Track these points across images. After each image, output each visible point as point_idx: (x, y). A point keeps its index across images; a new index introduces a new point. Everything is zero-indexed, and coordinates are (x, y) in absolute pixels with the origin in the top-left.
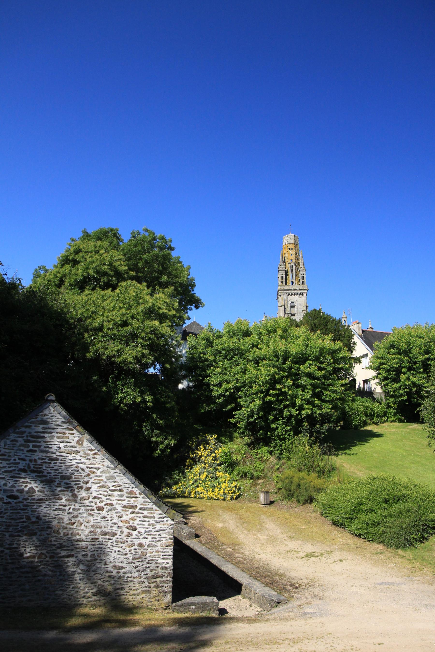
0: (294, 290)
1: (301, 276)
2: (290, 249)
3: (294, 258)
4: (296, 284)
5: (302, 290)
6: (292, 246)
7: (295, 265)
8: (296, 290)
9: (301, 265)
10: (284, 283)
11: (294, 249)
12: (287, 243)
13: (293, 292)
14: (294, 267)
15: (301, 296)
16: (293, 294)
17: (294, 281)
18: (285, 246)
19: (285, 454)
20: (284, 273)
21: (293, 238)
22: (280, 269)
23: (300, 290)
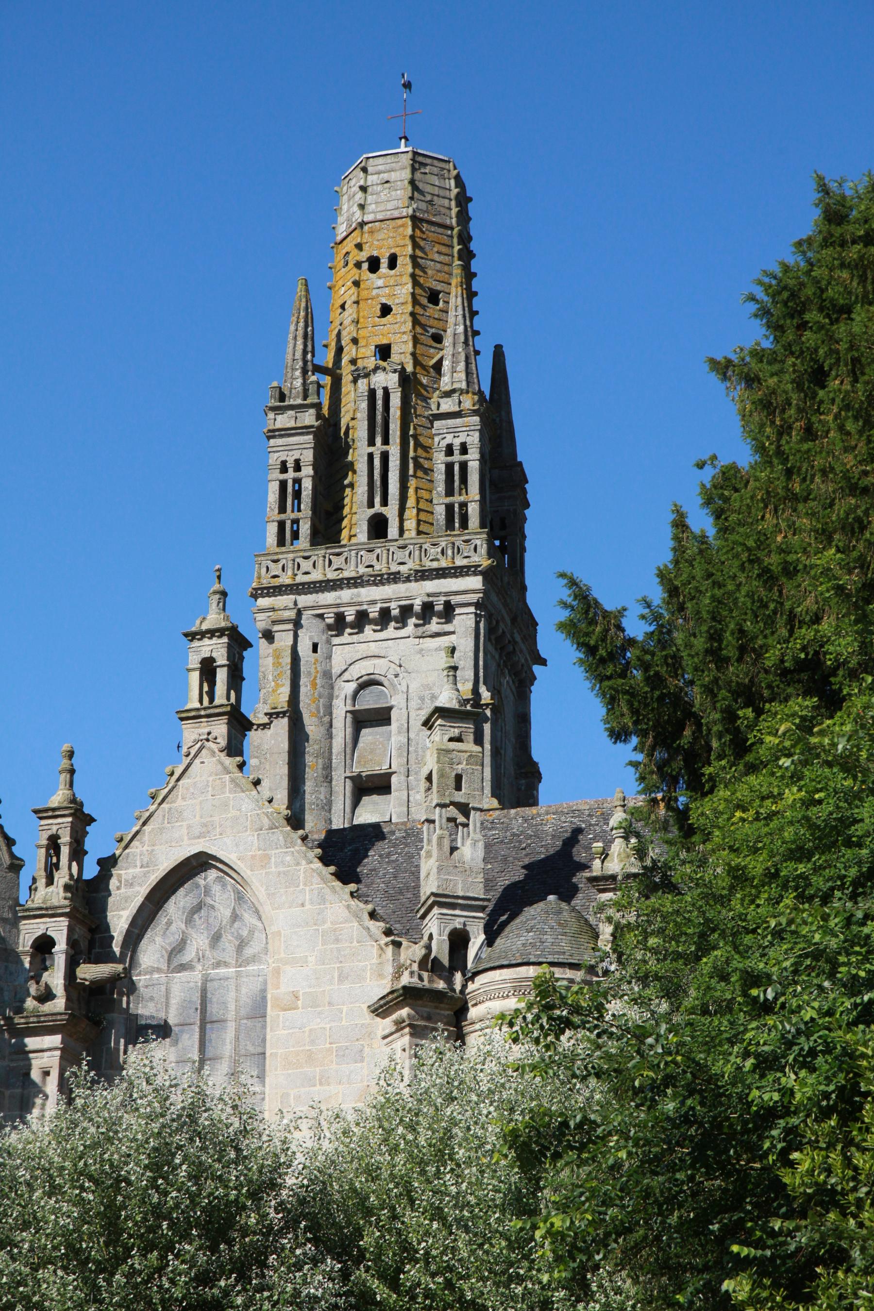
0: (379, 580)
1: (439, 460)
2: (374, 264)
5: (441, 573)
7: (406, 381)
8: (395, 578)
9: (446, 383)
10: (305, 528)
11: (405, 265)
12: (358, 216)
14: (396, 401)
15: (434, 625)
16: (374, 612)
17: (391, 512)
18: (349, 245)
20: (308, 456)
21: (406, 174)
22: (284, 420)
23: (423, 575)
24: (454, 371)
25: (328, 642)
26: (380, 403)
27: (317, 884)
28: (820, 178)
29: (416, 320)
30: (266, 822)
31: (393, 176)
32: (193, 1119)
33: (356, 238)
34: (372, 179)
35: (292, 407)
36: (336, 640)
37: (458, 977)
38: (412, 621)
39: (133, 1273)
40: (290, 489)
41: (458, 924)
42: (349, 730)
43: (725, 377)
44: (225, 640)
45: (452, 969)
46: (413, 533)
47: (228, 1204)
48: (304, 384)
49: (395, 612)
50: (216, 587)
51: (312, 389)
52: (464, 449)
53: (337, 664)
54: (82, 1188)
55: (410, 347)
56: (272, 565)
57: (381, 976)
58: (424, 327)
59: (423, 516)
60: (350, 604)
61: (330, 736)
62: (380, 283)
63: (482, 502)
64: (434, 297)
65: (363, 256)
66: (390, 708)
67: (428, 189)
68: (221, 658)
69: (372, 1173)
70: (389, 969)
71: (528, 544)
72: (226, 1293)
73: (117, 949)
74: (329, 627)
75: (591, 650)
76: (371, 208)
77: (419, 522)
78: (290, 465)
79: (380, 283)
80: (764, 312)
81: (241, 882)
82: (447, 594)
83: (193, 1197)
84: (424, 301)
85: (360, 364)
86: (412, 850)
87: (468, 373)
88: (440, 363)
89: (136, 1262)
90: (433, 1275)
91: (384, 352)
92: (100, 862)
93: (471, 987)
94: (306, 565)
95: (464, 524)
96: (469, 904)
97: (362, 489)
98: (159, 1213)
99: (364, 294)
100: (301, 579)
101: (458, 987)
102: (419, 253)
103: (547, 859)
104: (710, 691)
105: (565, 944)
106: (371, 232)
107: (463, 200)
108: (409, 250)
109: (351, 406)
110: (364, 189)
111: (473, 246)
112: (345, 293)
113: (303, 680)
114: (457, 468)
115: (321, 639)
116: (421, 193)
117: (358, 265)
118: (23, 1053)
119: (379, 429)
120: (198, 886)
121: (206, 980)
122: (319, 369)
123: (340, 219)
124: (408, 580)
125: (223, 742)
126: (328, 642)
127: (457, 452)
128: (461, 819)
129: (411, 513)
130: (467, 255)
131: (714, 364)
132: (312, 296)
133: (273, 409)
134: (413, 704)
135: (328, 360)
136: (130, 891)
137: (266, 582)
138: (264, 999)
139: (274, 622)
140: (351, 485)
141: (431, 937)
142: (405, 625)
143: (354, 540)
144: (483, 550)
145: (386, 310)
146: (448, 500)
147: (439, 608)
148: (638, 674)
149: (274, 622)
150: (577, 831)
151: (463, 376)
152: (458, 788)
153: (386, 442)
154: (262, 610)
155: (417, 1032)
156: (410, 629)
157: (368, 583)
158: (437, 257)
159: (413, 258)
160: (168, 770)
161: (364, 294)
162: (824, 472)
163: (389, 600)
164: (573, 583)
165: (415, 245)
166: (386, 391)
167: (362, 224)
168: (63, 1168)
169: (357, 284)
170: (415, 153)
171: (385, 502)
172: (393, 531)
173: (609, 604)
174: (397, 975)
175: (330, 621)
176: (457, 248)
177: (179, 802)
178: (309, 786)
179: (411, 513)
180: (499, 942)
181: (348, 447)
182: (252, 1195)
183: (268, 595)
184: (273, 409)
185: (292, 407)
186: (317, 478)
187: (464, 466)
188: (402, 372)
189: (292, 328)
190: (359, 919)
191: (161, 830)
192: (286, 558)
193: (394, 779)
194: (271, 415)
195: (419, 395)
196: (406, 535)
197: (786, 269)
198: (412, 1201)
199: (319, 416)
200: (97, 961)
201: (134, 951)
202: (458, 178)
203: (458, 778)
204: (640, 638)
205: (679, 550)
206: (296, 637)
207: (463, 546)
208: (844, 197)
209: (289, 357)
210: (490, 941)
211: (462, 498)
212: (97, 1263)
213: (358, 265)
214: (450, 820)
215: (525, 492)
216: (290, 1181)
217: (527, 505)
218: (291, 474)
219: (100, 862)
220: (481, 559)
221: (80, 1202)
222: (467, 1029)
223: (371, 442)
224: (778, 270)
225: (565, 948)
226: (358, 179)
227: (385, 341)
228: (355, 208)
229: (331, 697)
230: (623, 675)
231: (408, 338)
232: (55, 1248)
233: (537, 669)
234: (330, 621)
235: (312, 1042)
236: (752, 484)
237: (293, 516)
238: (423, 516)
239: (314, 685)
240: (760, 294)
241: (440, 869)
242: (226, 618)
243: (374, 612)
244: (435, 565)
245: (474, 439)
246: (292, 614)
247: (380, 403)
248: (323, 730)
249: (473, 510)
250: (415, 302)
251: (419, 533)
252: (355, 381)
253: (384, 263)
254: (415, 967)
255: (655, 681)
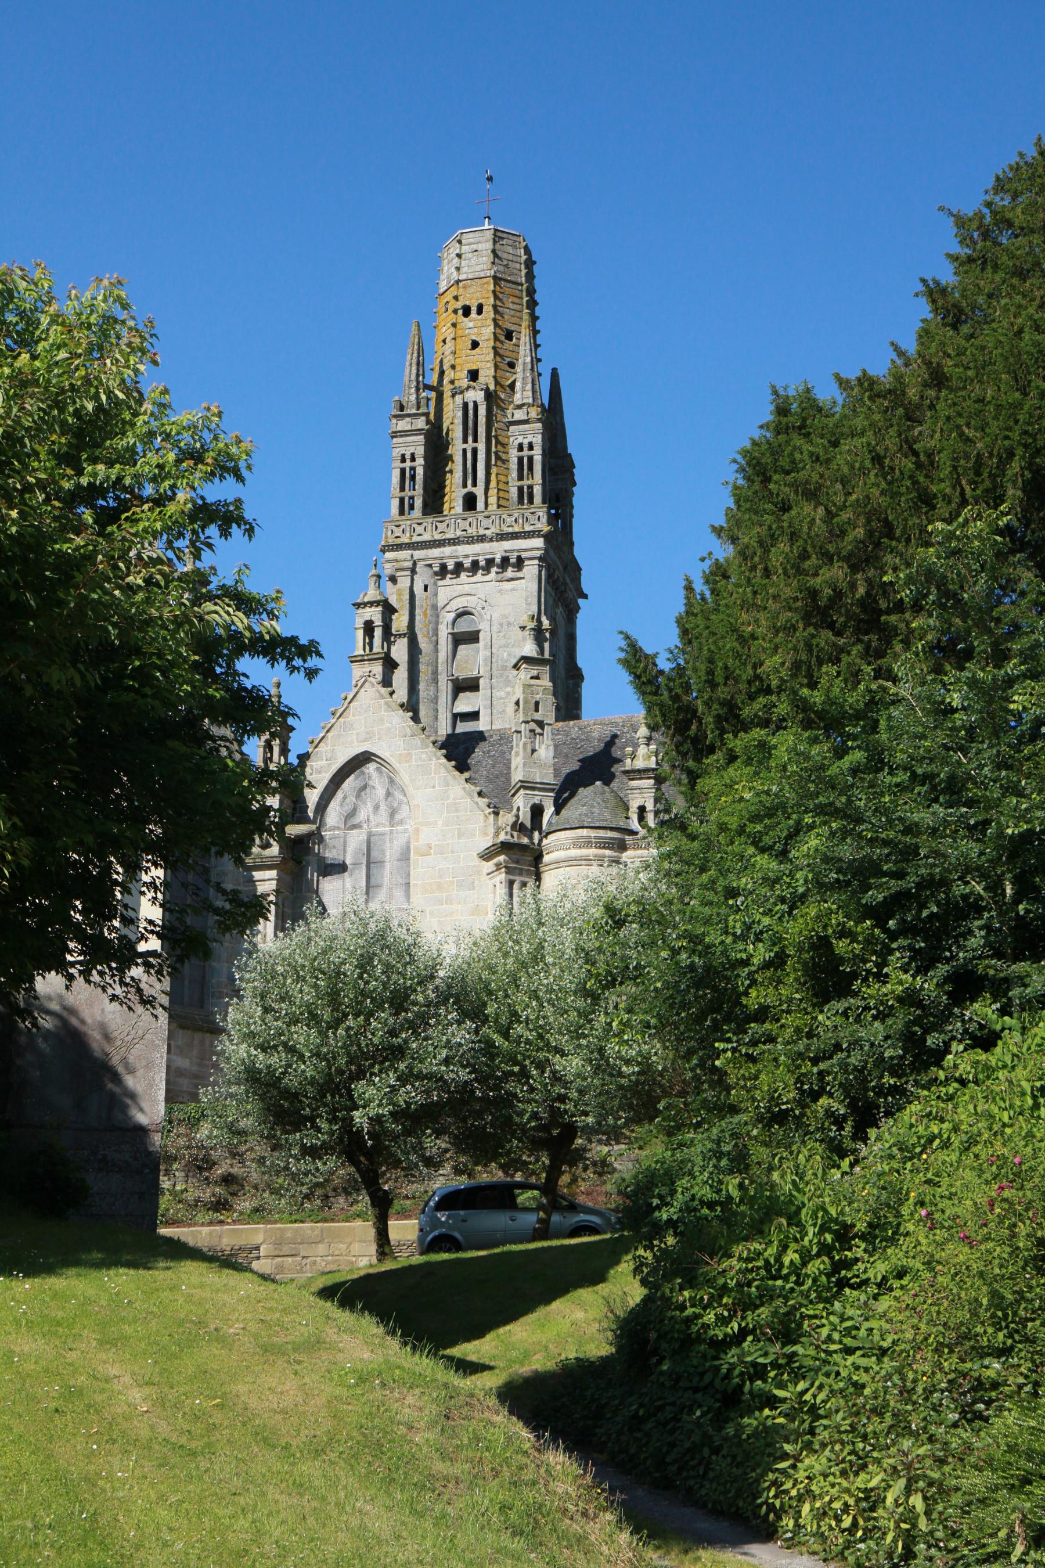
0: (471, 540)
1: (513, 455)
2: (467, 311)
3: (484, 361)
4: (493, 507)
5: (515, 536)
6: (481, 294)
7: (490, 396)
8: (482, 539)
9: (518, 398)
10: (418, 503)
11: (488, 312)
12: (455, 276)
13: (466, 552)
14: (482, 411)
15: (510, 573)
16: (467, 563)
17: (479, 491)
18: (449, 296)
19: (108, 1541)
20: (420, 451)
21: (489, 246)
22: (403, 425)
23: (502, 537)
24: (523, 390)
25: (435, 584)
26: (471, 412)
27: (443, 772)
28: (773, 387)
29: (496, 353)
30: (409, 731)
31: (480, 247)
32: (383, 937)
33: (454, 291)
34: (465, 249)
35: (409, 415)
36: (440, 583)
37: (536, 834)
38: (494, 569)
39: (349, 1028)
40: (407, 475)
41: (536, 800)
42: (450, 647)
43: (719, 537)
44: (380, 608)
45: (533, 829)
46: (495, 506)
47: (406, 988)
48: (417, 398)
49: (482, 563)
50: (374, 572)
51: (423, 402)
52: (531, 447)
53: (441, 600)
54: (318, 979)
55: (492, 372)
56: (395, 529)
57: (486, 834)
58: (502, 356)
59: (501, 494)
60: (450, 557)
61: (437, 651)
62: (471, 325)
63: (544, 485)
64: (509, 335)
65: (459, 305)
66: (478, 632)
67: (505, 256)
68: (378, 621)
69: (492, 969)
70: (491, 830)
71: (575, 512)
72: (406, 1041)
73: (311, 814)
74: (436, 574)
75: (638, 677)
76: (464, 270)
77: (499, 498)
78: (408, 457)
79: (471, 325)
80: (742, 470)
81: (394, 771)
82: (518, 551)
83: (384, 984)
84: (503, 338)
85: (457, 384)
86: (505, 748)
87: (534, 392)
88: (514, 382)
89: (350, 1022)
90: (531, 1031)
91: (474, 375)
92: (299, 757)
93: (545, 842)
94: (419, 529)
95: (531, 500)
96: (544, 787)
97: (458, 474)
98: (363, 994)
99: (460, 333)
100: (416, 539)
101: (536, 841)
102: (498, 303)
103: (595, 755)
104: (707, 704)
105: (607, 815)
106: (465, 287)
107: (530, 264)
108: (492, 301)
109: (450, 414)
110: (459, 256)
111: (537, 297)
112: (447, 331)
113: (418, 611)
114: (525, 460)
115: (429, 582)
116: (500, 259)
117: (455, 311)
118: (252, 882)
119: (470, 431)
120: (363, 773)
121: (370, 835)
122: (427, 387)
123: (442, 277)
124: (491, 540)
125: (380, 678)
126: (435, 584)
127: (525, 449)
128: (538, 730)
129: (493, 492)
130: (532, 304)
131: (713, 528)
132: (423, 334)
133: (395, 416)
134: (495, 629)
135: (433, 380)
136: (319, 776)
137: (391, 541)
138: (408, 848)
139: (397, 570)
140: (451, 472)
141: (518, 809)
142: (489, 572)
143: (453, 512)
144: (544, 519)
145: (475, 345)
146: (520, 483)
147: (513, 560)
148: (666, 693)
149: (397, 570)
150: (615, 737)
151: (530, 394)
152: (537, 710)
153: (475, 440)
154: (388, 561)
155: (509, 871)
156: (492, 575)
157: (463, 543)
158: (511, 306)
159: (495, 307)
160: (343, 695)
161: (460, 333)
162: (774, 597)
163: (478, 555)
164: (627, 637)
165: (496, 297)
166: (475, 404)
167: (458, 282)
168: (303, 966)
169: (454, 325)
170: (496, 230)
171: (475, 484)
172: (480, 505)
173: (649, 650)
174: (497, 834)
175: (437, 569)
176: (526, 299)
177: (351, 718)
178: (422, 686)
179: (493, 492)
180: (563, 812)
181: (448, 443)
182: (420, 983)
183: (393, 550)
184: (395, 416)
185: (409, 415)
186: (426, 467)
187: (531, 459)
188: (487, 391)
189: (409, 357)
190: (472, 797)
191: (339, 736)
192: (405, 524)
193: (481, 681)
194: (394, 421)
195: (499, 407)
196: (490, 508)
197: (754, 443)
198: (517, 986)
199: (428, 422)
200: (299, 822)
201: (322, 816)
202: (526, 248)
203: (537, 704)
204: (667, 670)
205: (689, 604)
206: (412, 580)
207: (530, 516)
208: (787, 397)
209: (407, 378)
210: (558, 812)
211: (530, 482)
212: (327, 1023)
213: (455, 311)
214: (532, 731)
215: (573, 474)
216: (441, 973)
217: (574, 484)
218: (408, 464)
219: (299, 757)
220: (543, 526)
221: (316, 986)
222: (542, 869)
223: (465, 441)
224: (748, 445)
225: (608, 817)
226: (455, 249)
227: (474, 368)
228: (453, 270)
229: (437, 623)
230: (656, 693)
231: (491, 365)
232: (301, 1014)
233: (581, 601)
234: (437, 569)
235: (441, 877)
236: (735, 596)
237: (410, 494)
238: (501, 494)
239: (425, 614)
240: (739, 458)
241: (525, 765)
242: (381, 594)
243: (467, 563)
244: (510, 530)
245: (538, 440)
246: (409, 564)
247: (471, 412)
248: (431, 647)
249: (537, 490)
250: (496, 338)
251: (499, 506)
252: (453, 396)
253: (474, 310)
254: (509, 829)
255: (676, 698)
